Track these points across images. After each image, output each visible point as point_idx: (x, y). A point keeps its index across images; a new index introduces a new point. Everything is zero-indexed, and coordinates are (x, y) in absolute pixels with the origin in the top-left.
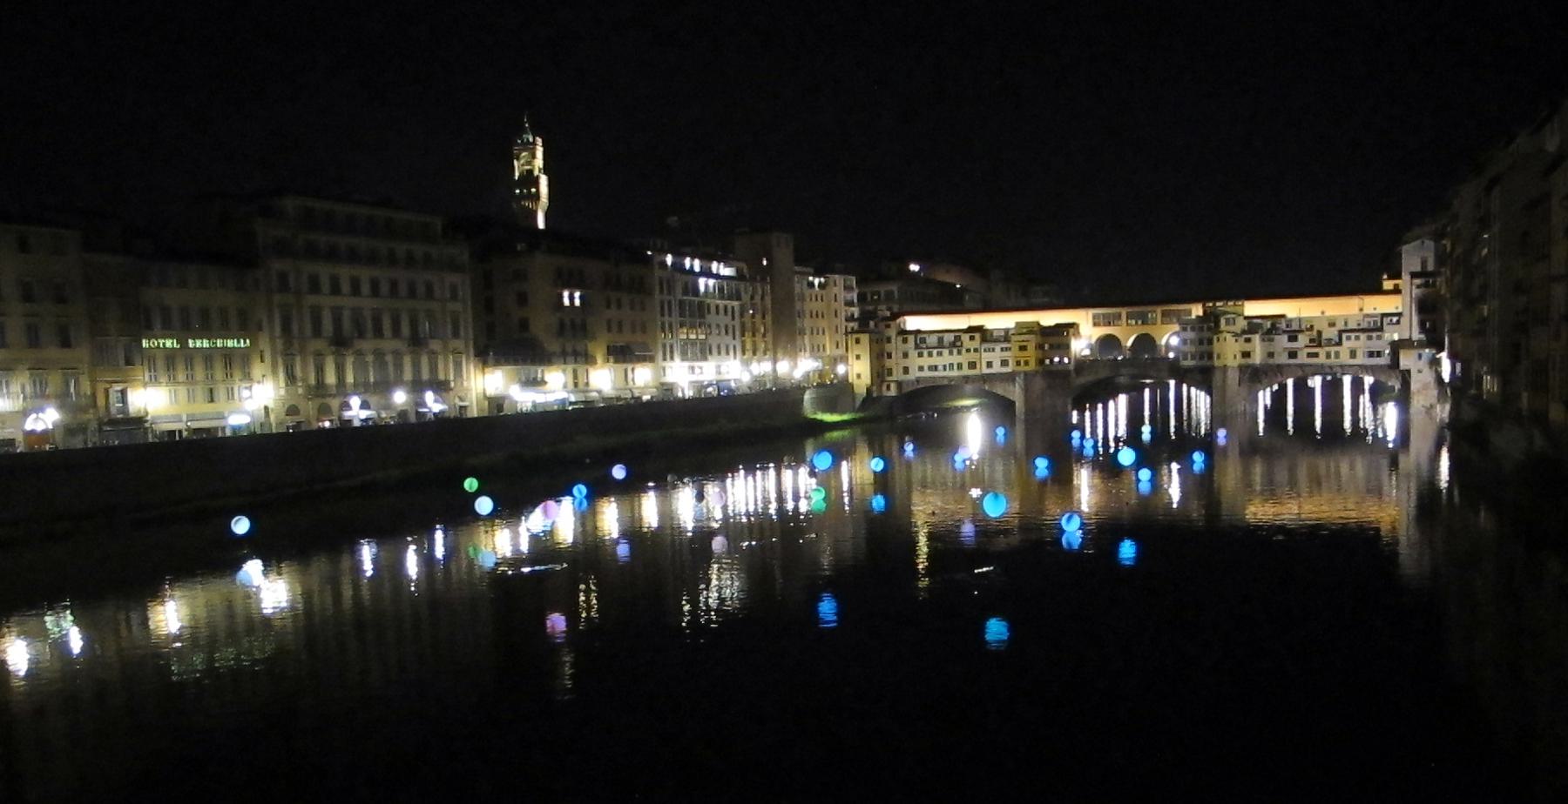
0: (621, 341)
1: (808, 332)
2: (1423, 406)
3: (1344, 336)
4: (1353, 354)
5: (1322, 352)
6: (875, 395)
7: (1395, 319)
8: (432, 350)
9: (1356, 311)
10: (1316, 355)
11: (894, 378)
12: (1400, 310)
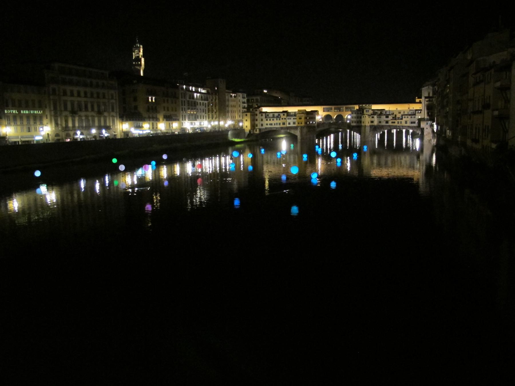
0: (168, 113)
1: (230, 112)
2: (428, 140)
3: (403, 116)
4: (406, 122)
5: (396, 121)
6: (252, 133)
7: (419, 112)
8: (104, 116)
9: (407, 109)
10: (394, 122)
11: (258, 127)
12: (421, 109)
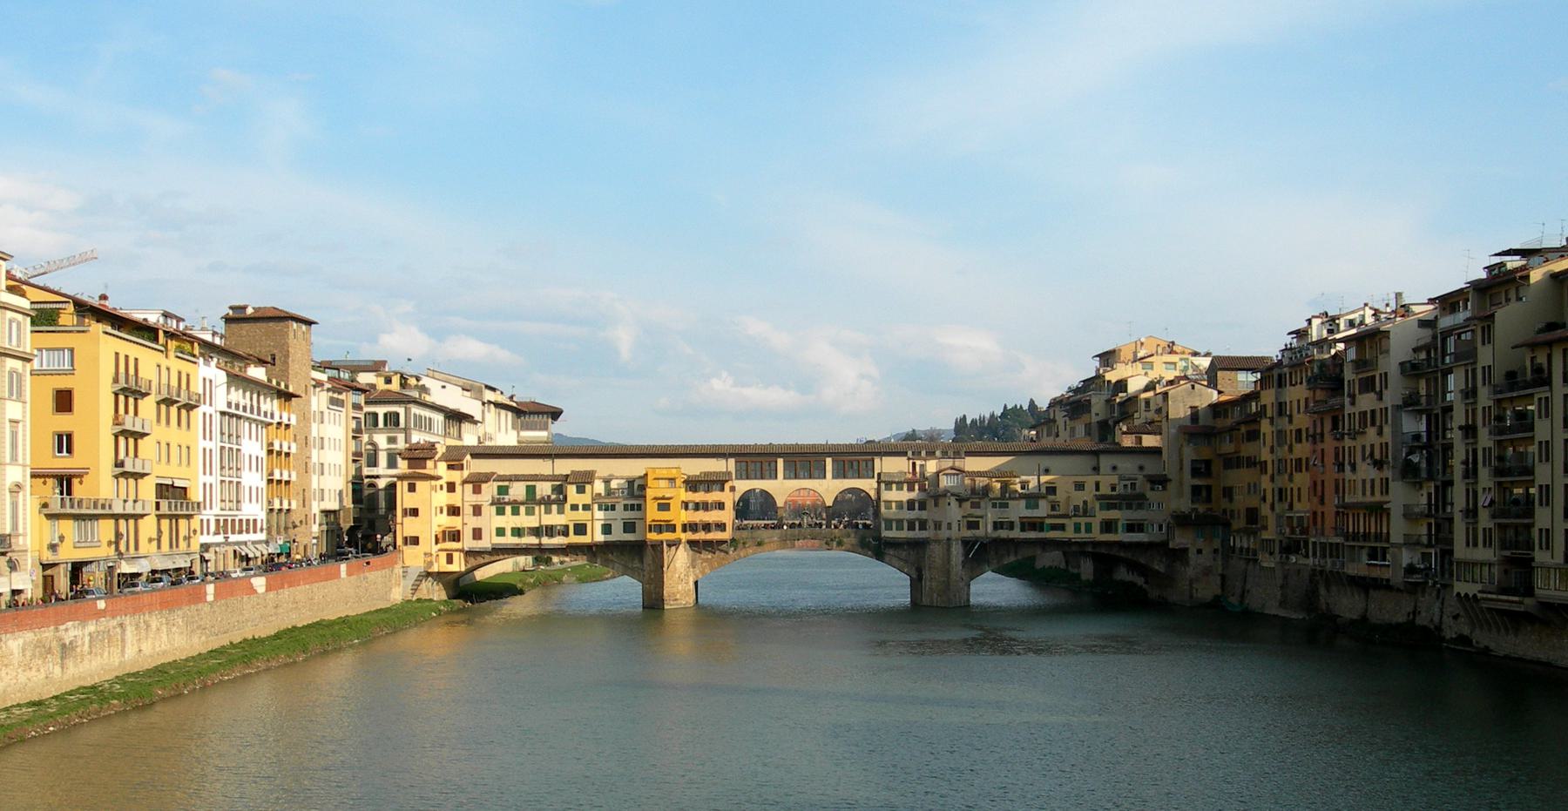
5: (1070, 523)
10: (1062, 527)
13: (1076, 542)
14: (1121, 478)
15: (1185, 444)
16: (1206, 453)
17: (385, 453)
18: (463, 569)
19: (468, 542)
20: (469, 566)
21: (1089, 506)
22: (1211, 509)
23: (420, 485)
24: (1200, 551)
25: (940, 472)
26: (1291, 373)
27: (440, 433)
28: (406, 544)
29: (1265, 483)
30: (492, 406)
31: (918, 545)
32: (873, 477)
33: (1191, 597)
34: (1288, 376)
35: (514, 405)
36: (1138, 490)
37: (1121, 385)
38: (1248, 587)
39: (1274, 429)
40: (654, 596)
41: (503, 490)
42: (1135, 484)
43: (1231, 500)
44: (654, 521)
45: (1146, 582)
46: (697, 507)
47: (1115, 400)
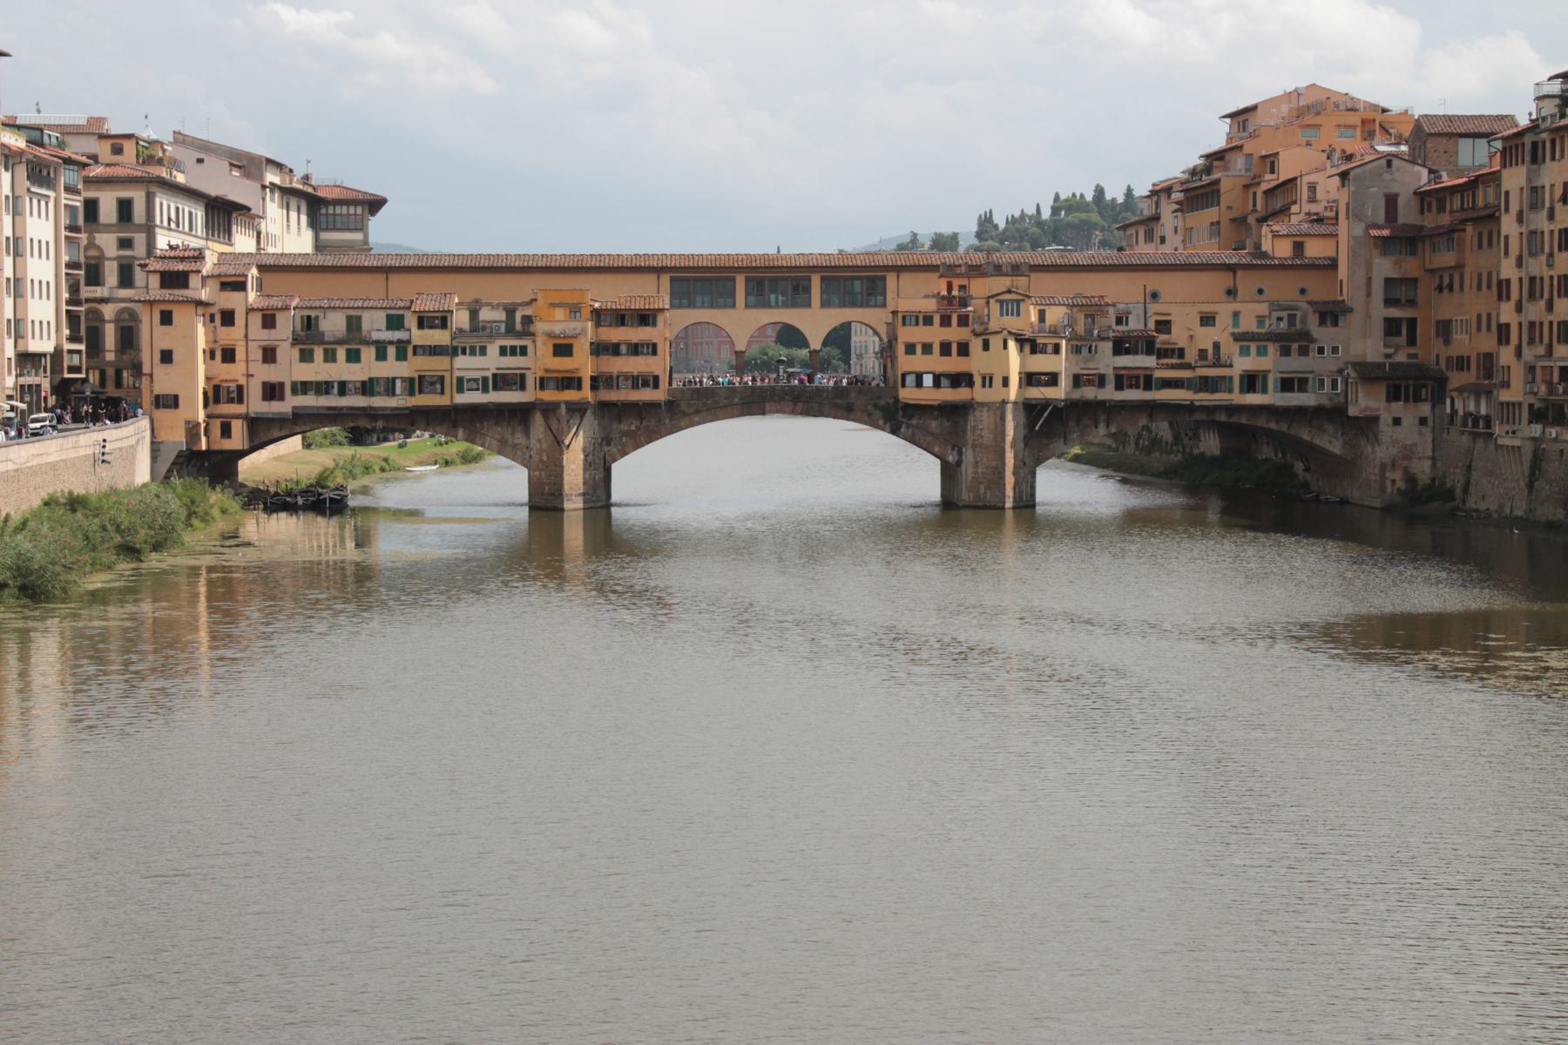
13: (1202, 406)
14: (1275, 306)
15: (1376, 252)
16: (1411, 267)
17: (115, 264)
18: (246, 447)
19: (256, 404)
20: (256, 442)
21: (1223, 351)
22: (1415, 356)
23: (179, 315)
24: (1397, 421)
25: (992, 297)
26: (1553, 142)
27: (199, 233)
28: (157, 406)
29: (1507, 313)
30: (277, 190)
31: (956, 412)
32: (884, 305)
33: (1383, 489)
34: (1548, 145)
35: (310, 190)
36: (1298, 326)
37: (1270, 161)
38: (1475, 476)
39: (1524, 229)
40: (547, 488)
41: (309, 323)
42: (1295, 315)
43: (1447, 342)
44: (547, 371)
45: (1307, 470)
46: (614, 349)
47: (1259, 183)
